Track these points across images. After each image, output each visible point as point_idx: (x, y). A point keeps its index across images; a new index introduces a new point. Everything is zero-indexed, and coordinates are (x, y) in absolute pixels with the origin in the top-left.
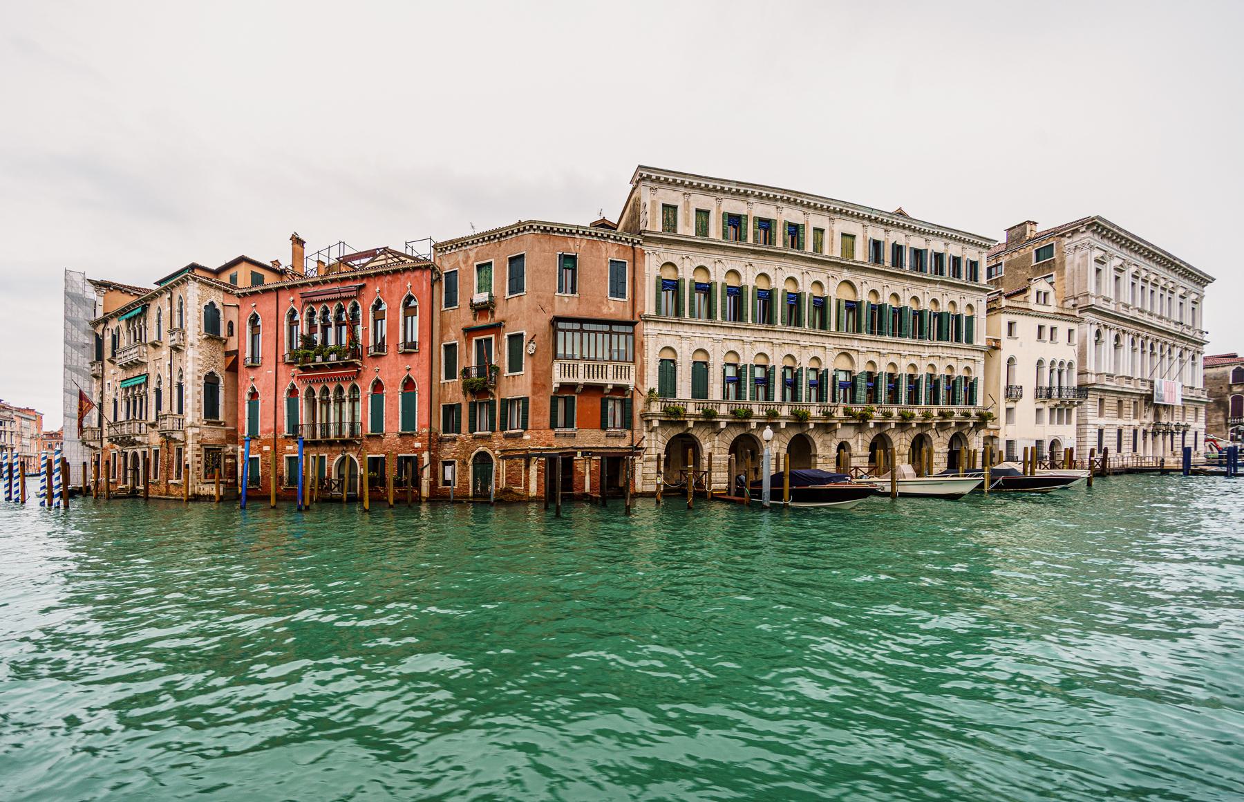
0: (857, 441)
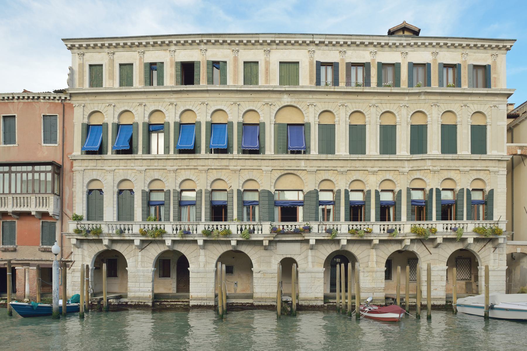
0: (306, 257)
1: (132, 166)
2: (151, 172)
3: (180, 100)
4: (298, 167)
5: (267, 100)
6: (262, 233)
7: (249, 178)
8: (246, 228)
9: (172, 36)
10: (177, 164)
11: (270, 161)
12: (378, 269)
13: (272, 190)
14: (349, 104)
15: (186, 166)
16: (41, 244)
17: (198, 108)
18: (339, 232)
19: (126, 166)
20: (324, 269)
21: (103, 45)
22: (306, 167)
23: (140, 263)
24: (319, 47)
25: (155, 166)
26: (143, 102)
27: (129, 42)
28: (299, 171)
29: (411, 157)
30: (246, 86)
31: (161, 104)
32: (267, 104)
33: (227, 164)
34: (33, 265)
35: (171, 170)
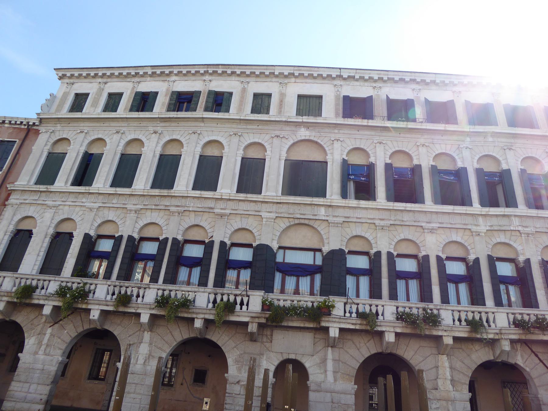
0: (324, 361)
1: (82, 202)
2: (106, 211)
3: (166, 129)
4: (316, 215)
5: (278, 133)
6: (247, 309)
7: (240, 227)
8: (222, 300)
9: (174, 67)
10: (142, 202)
11: (275, 205)
12: (457, 395)
13: (275, 246)
14: (389, 143)
15: (155, 205)
17: (187, 138)
18: (381, 317)
19: (75, 202)
21: (96, 75)
22: (327, 216)
24: (347, 83)
25: (113, 203)
26: (121, 130)
27: (125, 73)
28: (317, 221)
29: (487, 212)
30: (252, 115)
31: (143, 132)
32: (278, 136)
33: (212, 206)
35: (133, 209)
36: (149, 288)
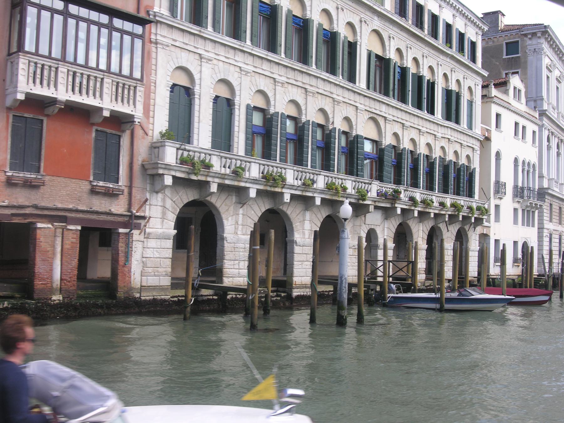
1: (236, 61)
16: (91, 179)
20: (394, 245)
23: (240, 227)
25: (263, 69)
34: (75, 221)
35: (281, 81)
36: (320, 174)
